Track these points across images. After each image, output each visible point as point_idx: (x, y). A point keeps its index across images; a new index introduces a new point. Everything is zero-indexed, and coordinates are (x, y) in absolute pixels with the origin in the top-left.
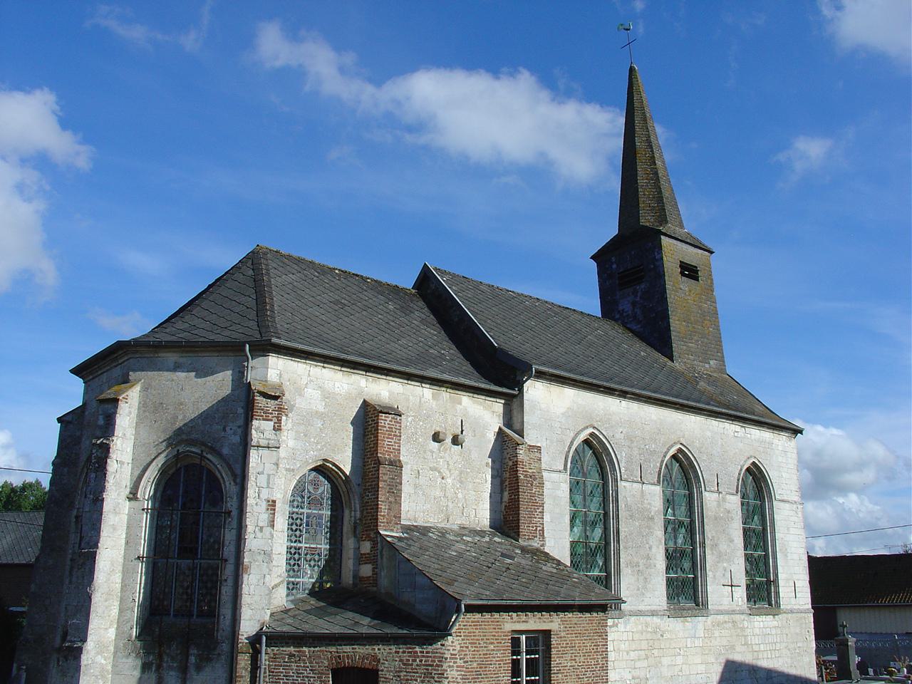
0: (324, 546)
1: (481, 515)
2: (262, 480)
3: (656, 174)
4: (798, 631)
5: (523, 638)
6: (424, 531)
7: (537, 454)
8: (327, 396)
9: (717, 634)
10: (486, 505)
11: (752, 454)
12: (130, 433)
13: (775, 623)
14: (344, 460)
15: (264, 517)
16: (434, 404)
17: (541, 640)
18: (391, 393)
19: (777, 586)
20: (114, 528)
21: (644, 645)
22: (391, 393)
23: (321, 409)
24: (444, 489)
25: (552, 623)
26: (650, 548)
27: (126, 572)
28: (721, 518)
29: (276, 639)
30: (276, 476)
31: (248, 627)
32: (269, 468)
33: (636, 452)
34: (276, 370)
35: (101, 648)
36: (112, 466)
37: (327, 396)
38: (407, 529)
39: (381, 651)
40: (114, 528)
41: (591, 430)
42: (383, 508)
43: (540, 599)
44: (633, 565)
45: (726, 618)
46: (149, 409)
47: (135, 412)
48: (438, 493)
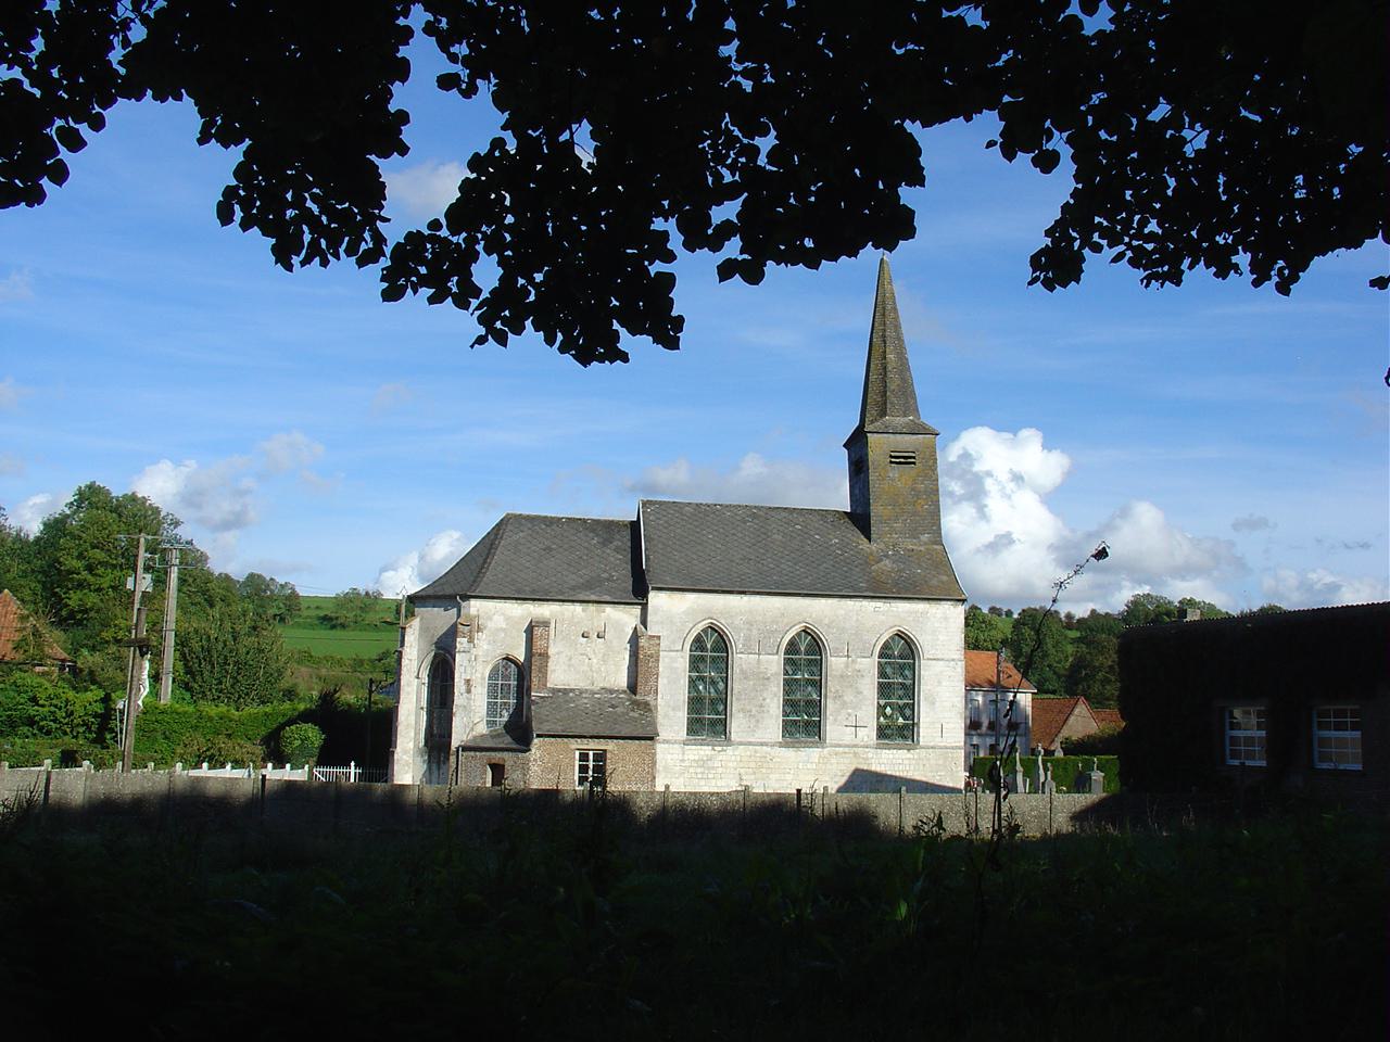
0: (513, 701)
1: (622, 681)
2: (462, 669)
3: (885, 368)
4: (941, 762)
5: (591, 753)
6: (565, 692)
7: (657, 642)
8: (508, 619)
9: (833, 761)
10: (626, 679)
11: (897, 623)
12: (415, 644)
13: (909, 756)
14: (520, 655)
15: (463, 688)
16: (583, 614)
17: (601, 756)
18: (551, 612)
19: (919, 728)
20: (409, 693)
21: (753, 765)
22: (551, 612)
23: (504, 626)
24: (590, 666)
25: (610, 746)
26: (764, 700)
27: (417, 715)
28: (848, 676)
29: (465, 749)
30: (474, 670)
31: (455, 743)
32: (466, 663)
33: (755, 632)
34: (475, 607)
35: (405, 752)
36: (405, 662)
37: (508, 619)
38: (555, 691)
39: (506, 755)
40: (409, 693)
41: (710, 621)
42: (535, 680)
43: (607, 733)
44: (747, 713)
45: (847, 750)
46: (424, 630)
47: (417, 633)
48: (586, 668)
